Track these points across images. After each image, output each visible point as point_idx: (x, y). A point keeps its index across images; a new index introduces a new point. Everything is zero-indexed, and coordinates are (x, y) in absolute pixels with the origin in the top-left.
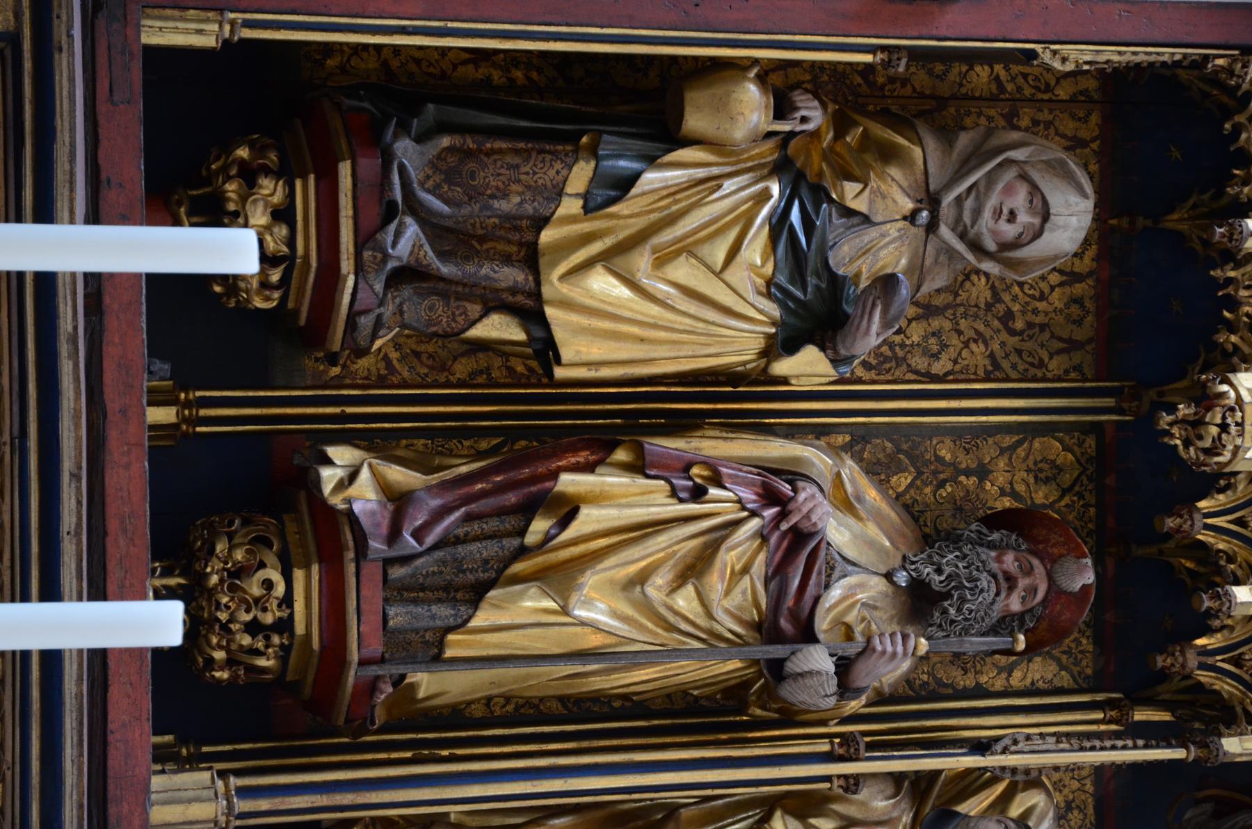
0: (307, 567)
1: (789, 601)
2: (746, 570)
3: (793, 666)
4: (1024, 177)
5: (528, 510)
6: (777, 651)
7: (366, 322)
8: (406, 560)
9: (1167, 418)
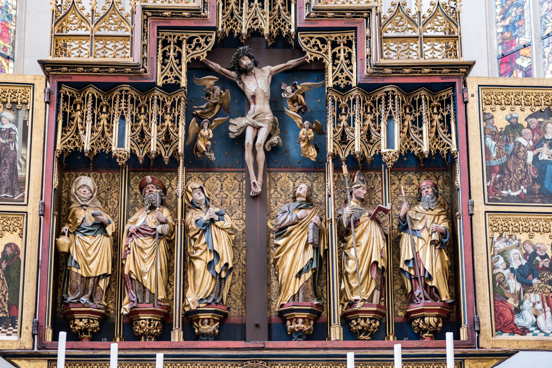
0: (139, 316)
1: (149, 233)
2: (142, 241)
3: (160, 232)
4: (78, 189)
5: (131, 279)
6: (157, 235)
7: (98, 306)
8: (138, 300)
9: (119, 164)
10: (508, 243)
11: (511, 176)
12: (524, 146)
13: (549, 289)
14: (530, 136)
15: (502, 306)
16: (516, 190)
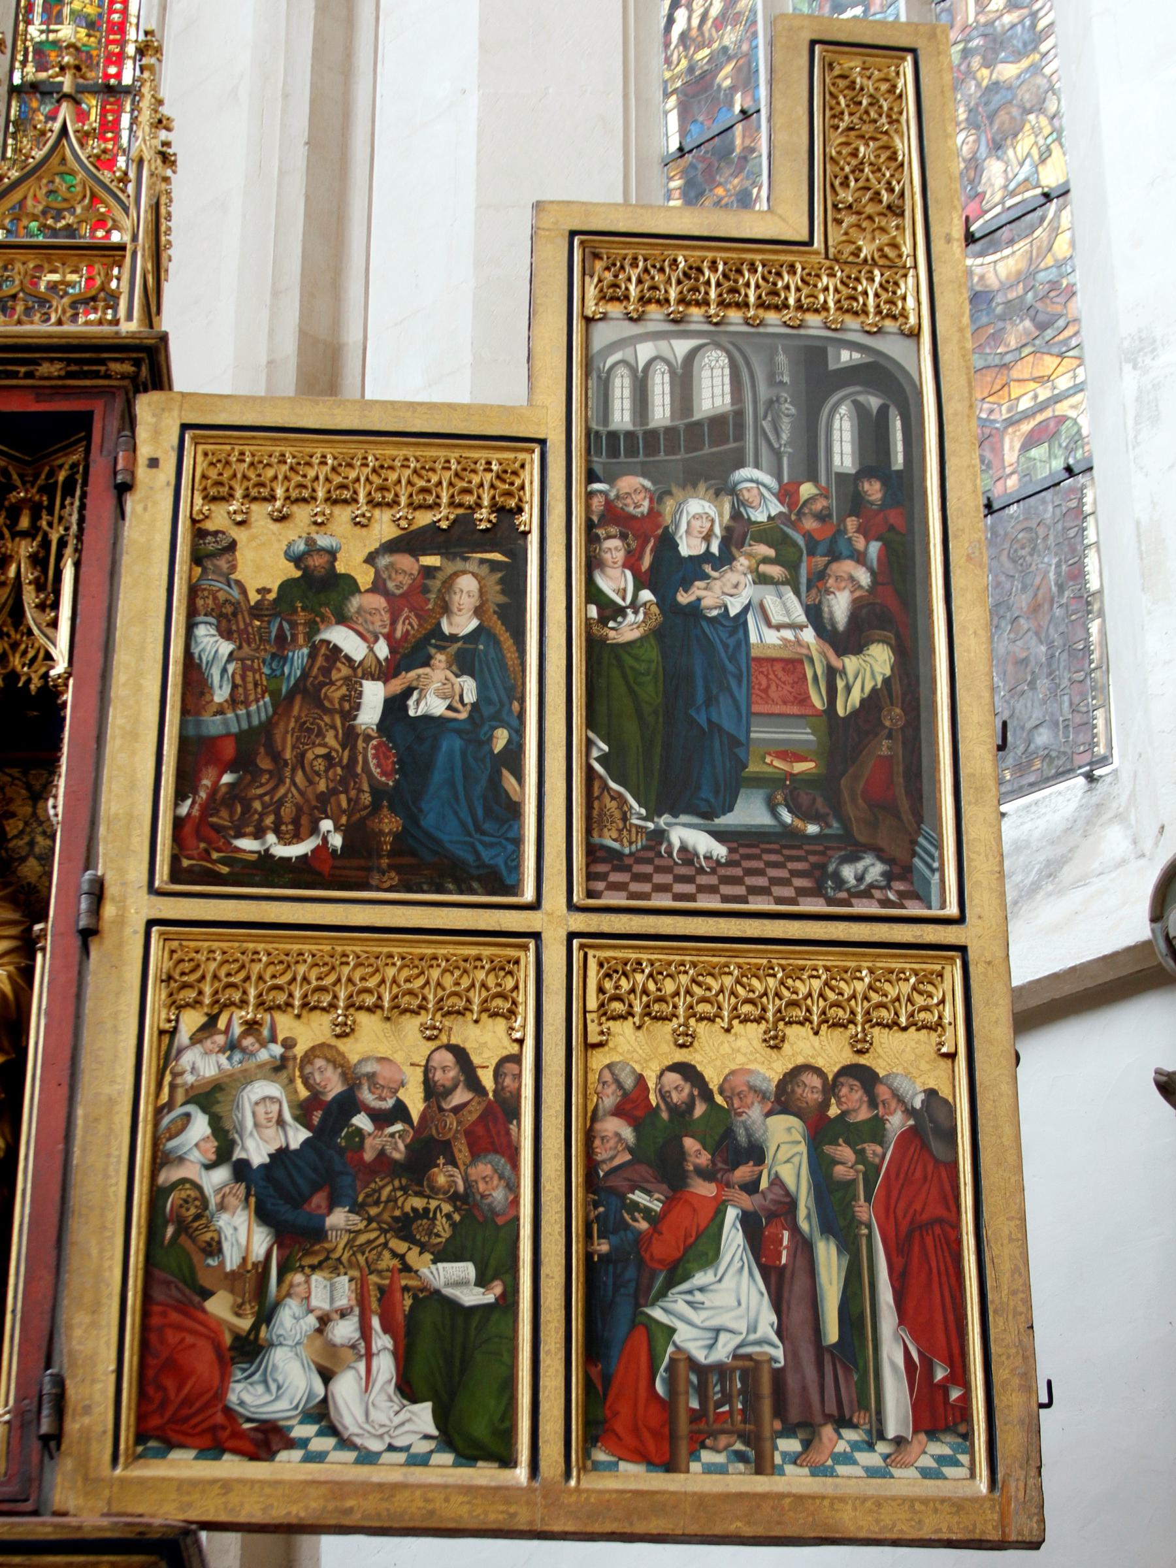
10: (237, 1056)
11: (281, 781)
12: (349, 659)
13: (395, 1255)
14: (380, 623)
15: (179, 1328)
16: (297, 838)
